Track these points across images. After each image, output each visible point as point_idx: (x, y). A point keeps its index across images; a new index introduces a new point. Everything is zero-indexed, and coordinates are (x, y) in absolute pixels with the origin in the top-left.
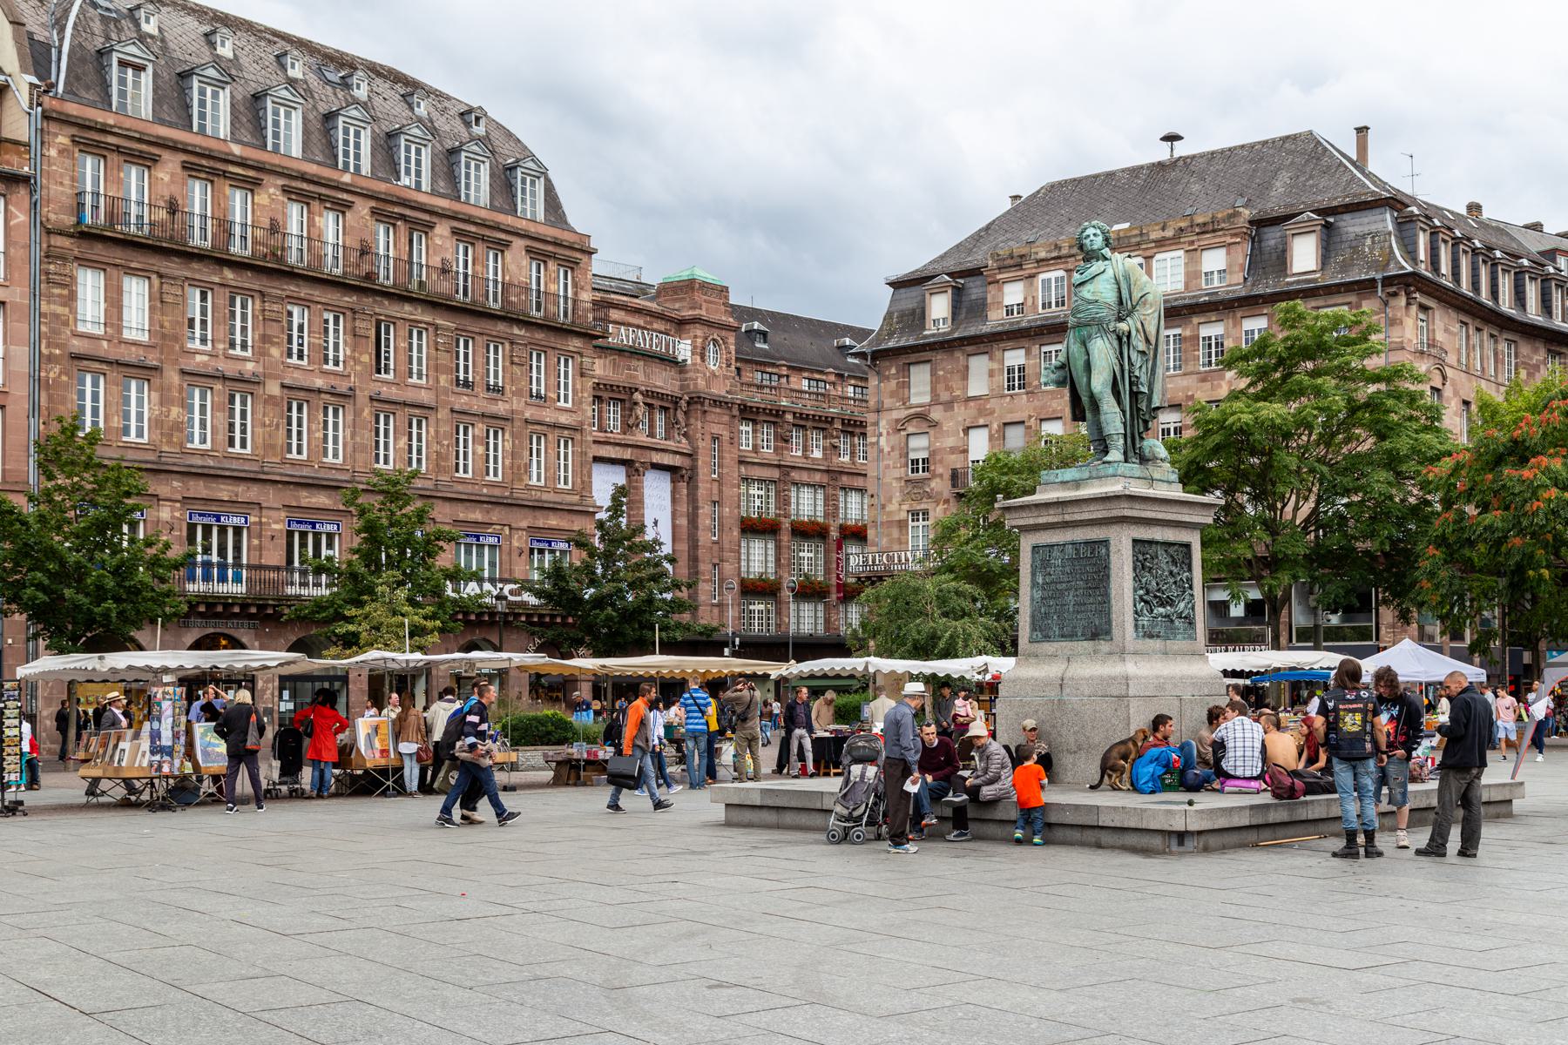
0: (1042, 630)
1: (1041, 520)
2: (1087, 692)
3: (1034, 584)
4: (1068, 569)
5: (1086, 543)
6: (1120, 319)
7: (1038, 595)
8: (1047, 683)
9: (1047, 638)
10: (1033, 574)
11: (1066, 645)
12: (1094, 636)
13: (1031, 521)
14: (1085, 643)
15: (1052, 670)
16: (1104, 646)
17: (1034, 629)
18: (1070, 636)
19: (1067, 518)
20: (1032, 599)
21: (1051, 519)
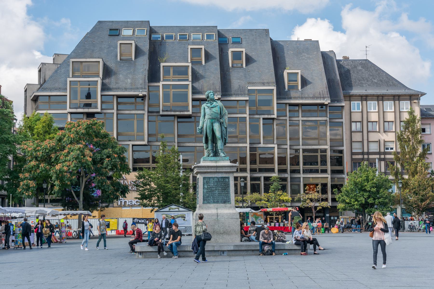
0: (206, 200)
1: (209, 171)
2: (226, 217)
5: (222, 178)
6: (220, 118)
7: (205, 191)
8: (213, 215)
9: (209, 203)
10: (204, 185)
11: (216, 205)
12: (225, 202)
13: (205, 171)
14: (222, 204)
15: (214, 211)
16: (228, 205)
17: (204, 200)
18: (217, 202)
19: (218, 171)
20: (204, 192)
21: (212, 171)
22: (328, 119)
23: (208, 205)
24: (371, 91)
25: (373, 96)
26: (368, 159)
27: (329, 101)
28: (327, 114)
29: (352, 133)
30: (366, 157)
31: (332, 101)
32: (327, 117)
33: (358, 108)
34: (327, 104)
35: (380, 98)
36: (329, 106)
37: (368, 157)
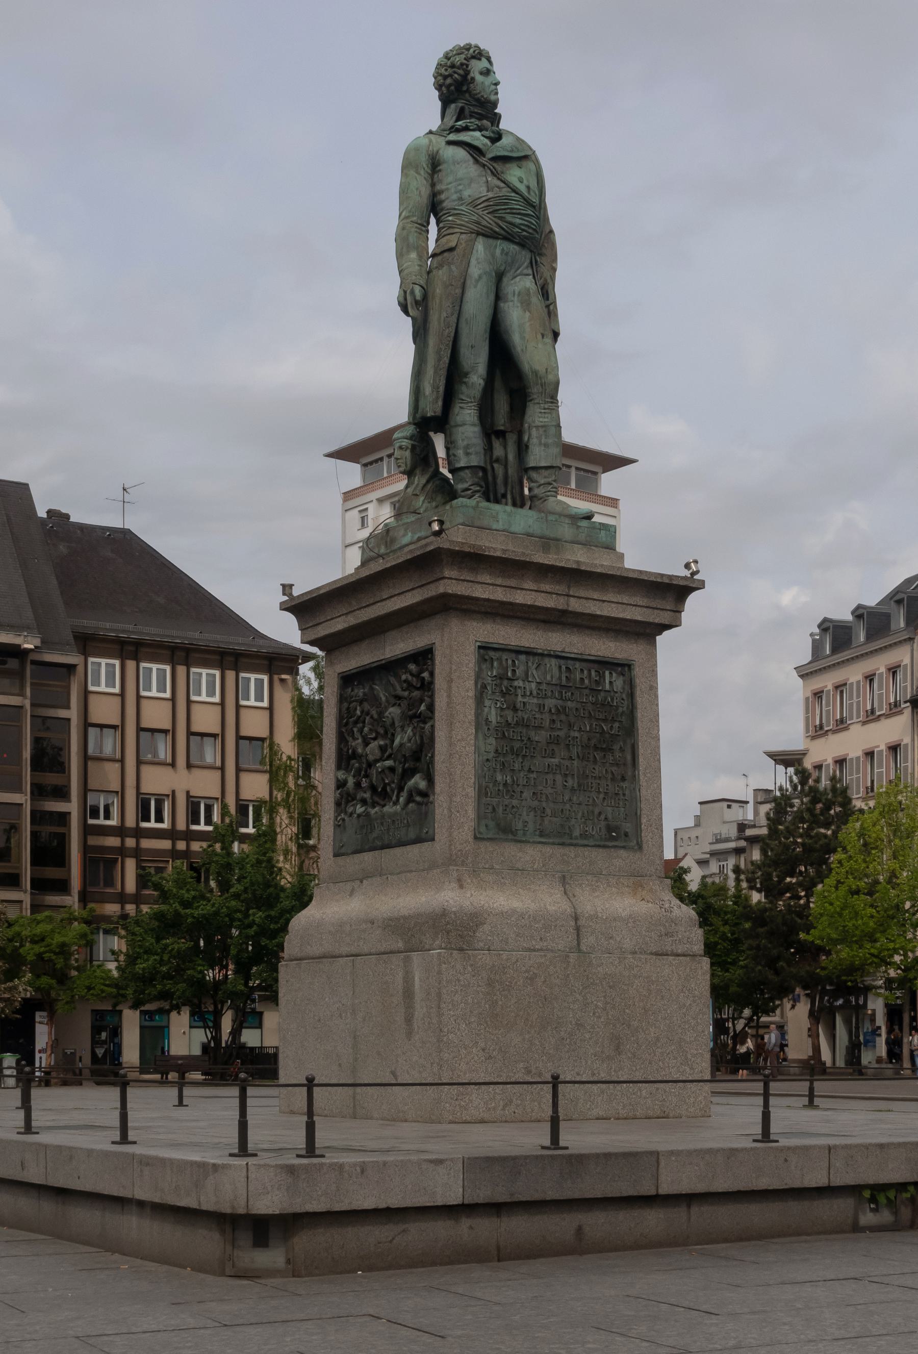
3: (481, 722)
4: (550, 703)
19: (575, 605)
21: (542, 601)
22: (27, 704)
23: (510, 850)
24: (150, 631)
25: (160, 645)
26: (137, 853)
27: (38, 642)
28: (22, 687)
29: (90, 763)
30: (130, 842)
31: (47, 644)
32: (22, 694)
33: (110, 682)
34: (31, 650)
35: (182, 655)
36: (34, 662)
37: (138, 843)
